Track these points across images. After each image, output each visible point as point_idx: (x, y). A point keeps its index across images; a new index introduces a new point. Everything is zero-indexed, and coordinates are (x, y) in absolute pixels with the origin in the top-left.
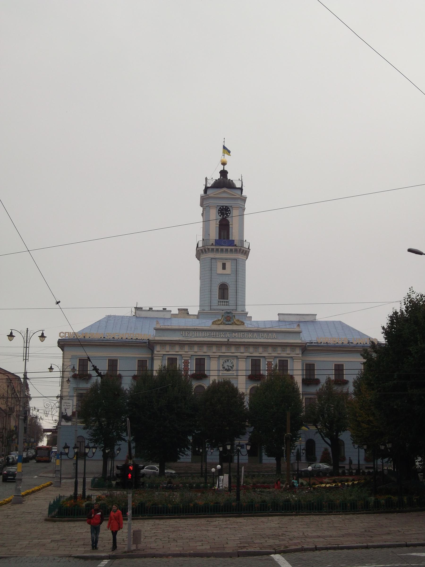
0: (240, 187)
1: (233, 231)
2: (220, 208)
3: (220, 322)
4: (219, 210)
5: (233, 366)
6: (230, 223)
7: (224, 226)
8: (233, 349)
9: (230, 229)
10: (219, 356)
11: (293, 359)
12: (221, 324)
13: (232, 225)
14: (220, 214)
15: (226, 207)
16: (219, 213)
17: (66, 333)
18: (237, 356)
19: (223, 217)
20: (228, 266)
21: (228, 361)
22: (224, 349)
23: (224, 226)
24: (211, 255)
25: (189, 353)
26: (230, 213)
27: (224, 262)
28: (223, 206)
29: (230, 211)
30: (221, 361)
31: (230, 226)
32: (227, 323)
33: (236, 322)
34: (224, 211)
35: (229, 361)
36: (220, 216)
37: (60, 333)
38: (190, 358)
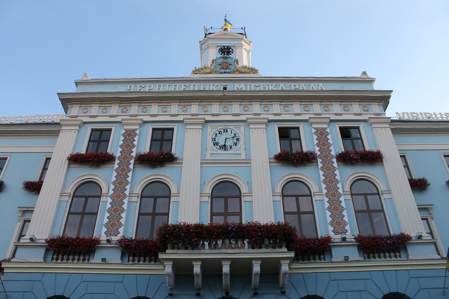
0: (244, 33)
2: (221, 48)
3: (208, 71)
4: (219, 50)
5: (238, 140)
8: (236, 108)
10: (207, 122)
11: (371, 124)
12: (210, 73)
14: (221, 53)
15: (227, 47)
16: (219, 52)
21: (226, 131)
22: (215, 108)
26: (232, 52)
28: (224, 47)
30: (211, 130)
32: (223, 71)
33: (240, 69)
35: (229, 131)
36: (221, 54)
38: (140, 125)
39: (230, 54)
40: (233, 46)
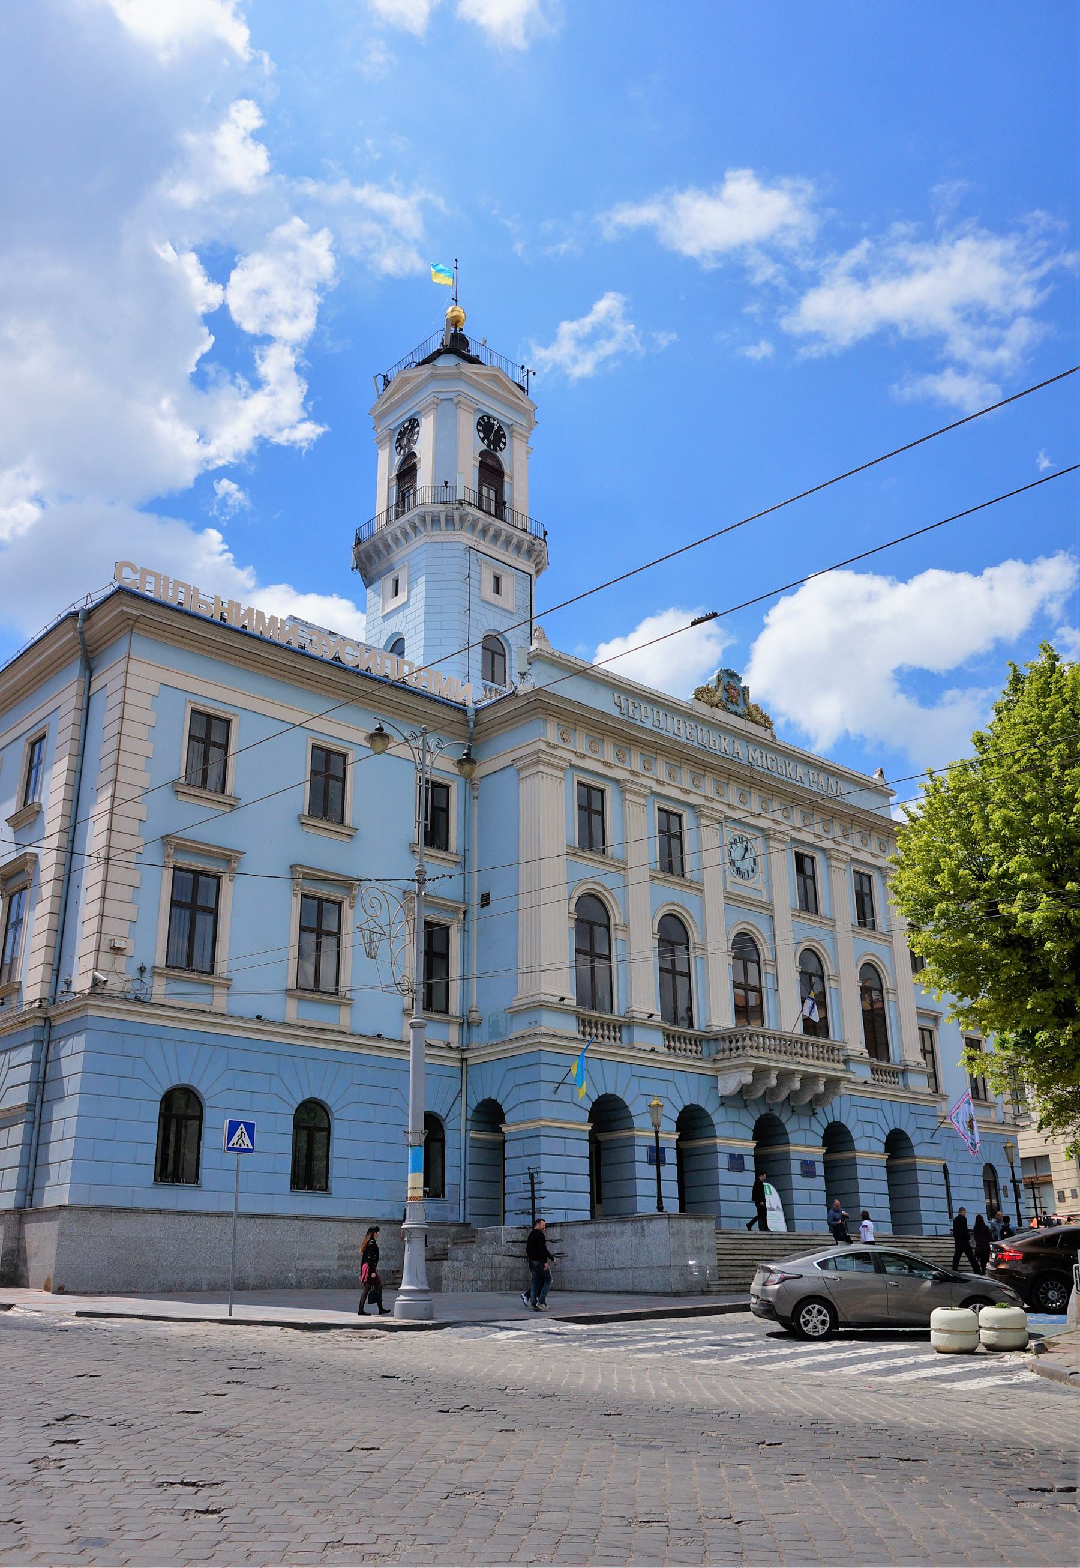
1: (516, 496)
2: (482, 418)
3: (715, 699)
4: (479, 423)
6: (506, 470)
7: (491, 472)
9: (506, 487)
13: (512, 478)
14: (482, 434)
16: (479, 431)
17: (145, 572)
18: (762, 830)
19: (489, 446)
20: (506, 584)
23: (491, 472)
24: (466, 538)
25: (642, 780)
27: (499, 572)
29: (504, 436)
31: (506, 478)
34: (491, 432)
36: (483, 440)
37: (119, 566)
39: (501, 450)
40: (508, 426)
